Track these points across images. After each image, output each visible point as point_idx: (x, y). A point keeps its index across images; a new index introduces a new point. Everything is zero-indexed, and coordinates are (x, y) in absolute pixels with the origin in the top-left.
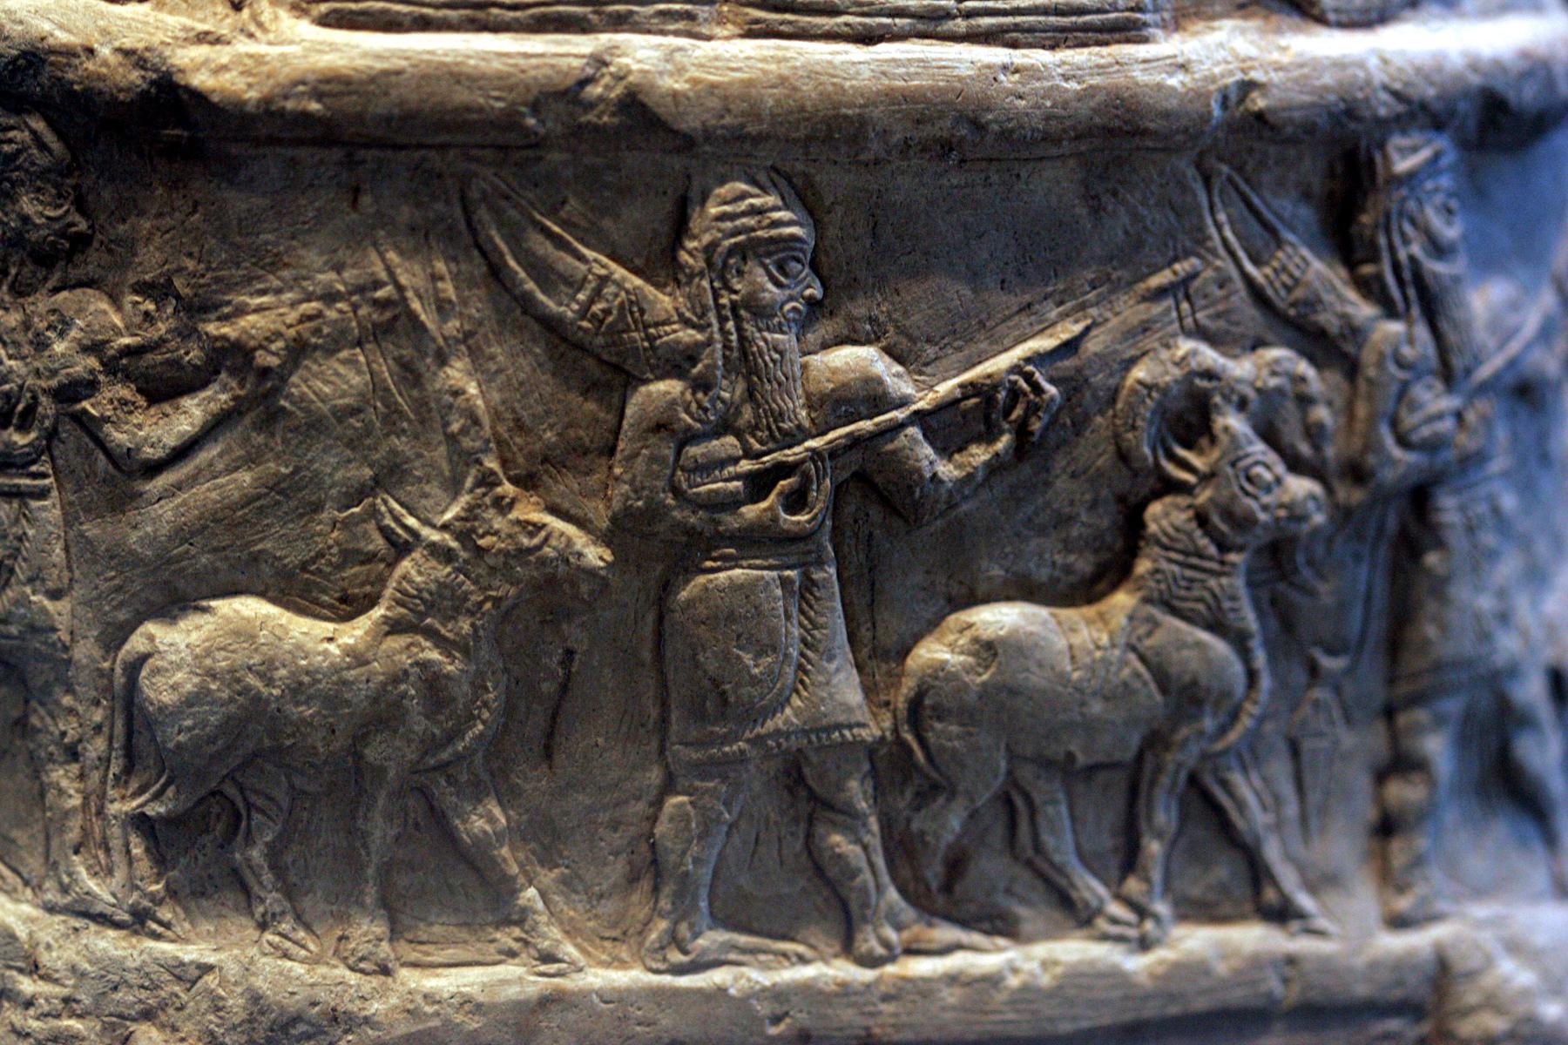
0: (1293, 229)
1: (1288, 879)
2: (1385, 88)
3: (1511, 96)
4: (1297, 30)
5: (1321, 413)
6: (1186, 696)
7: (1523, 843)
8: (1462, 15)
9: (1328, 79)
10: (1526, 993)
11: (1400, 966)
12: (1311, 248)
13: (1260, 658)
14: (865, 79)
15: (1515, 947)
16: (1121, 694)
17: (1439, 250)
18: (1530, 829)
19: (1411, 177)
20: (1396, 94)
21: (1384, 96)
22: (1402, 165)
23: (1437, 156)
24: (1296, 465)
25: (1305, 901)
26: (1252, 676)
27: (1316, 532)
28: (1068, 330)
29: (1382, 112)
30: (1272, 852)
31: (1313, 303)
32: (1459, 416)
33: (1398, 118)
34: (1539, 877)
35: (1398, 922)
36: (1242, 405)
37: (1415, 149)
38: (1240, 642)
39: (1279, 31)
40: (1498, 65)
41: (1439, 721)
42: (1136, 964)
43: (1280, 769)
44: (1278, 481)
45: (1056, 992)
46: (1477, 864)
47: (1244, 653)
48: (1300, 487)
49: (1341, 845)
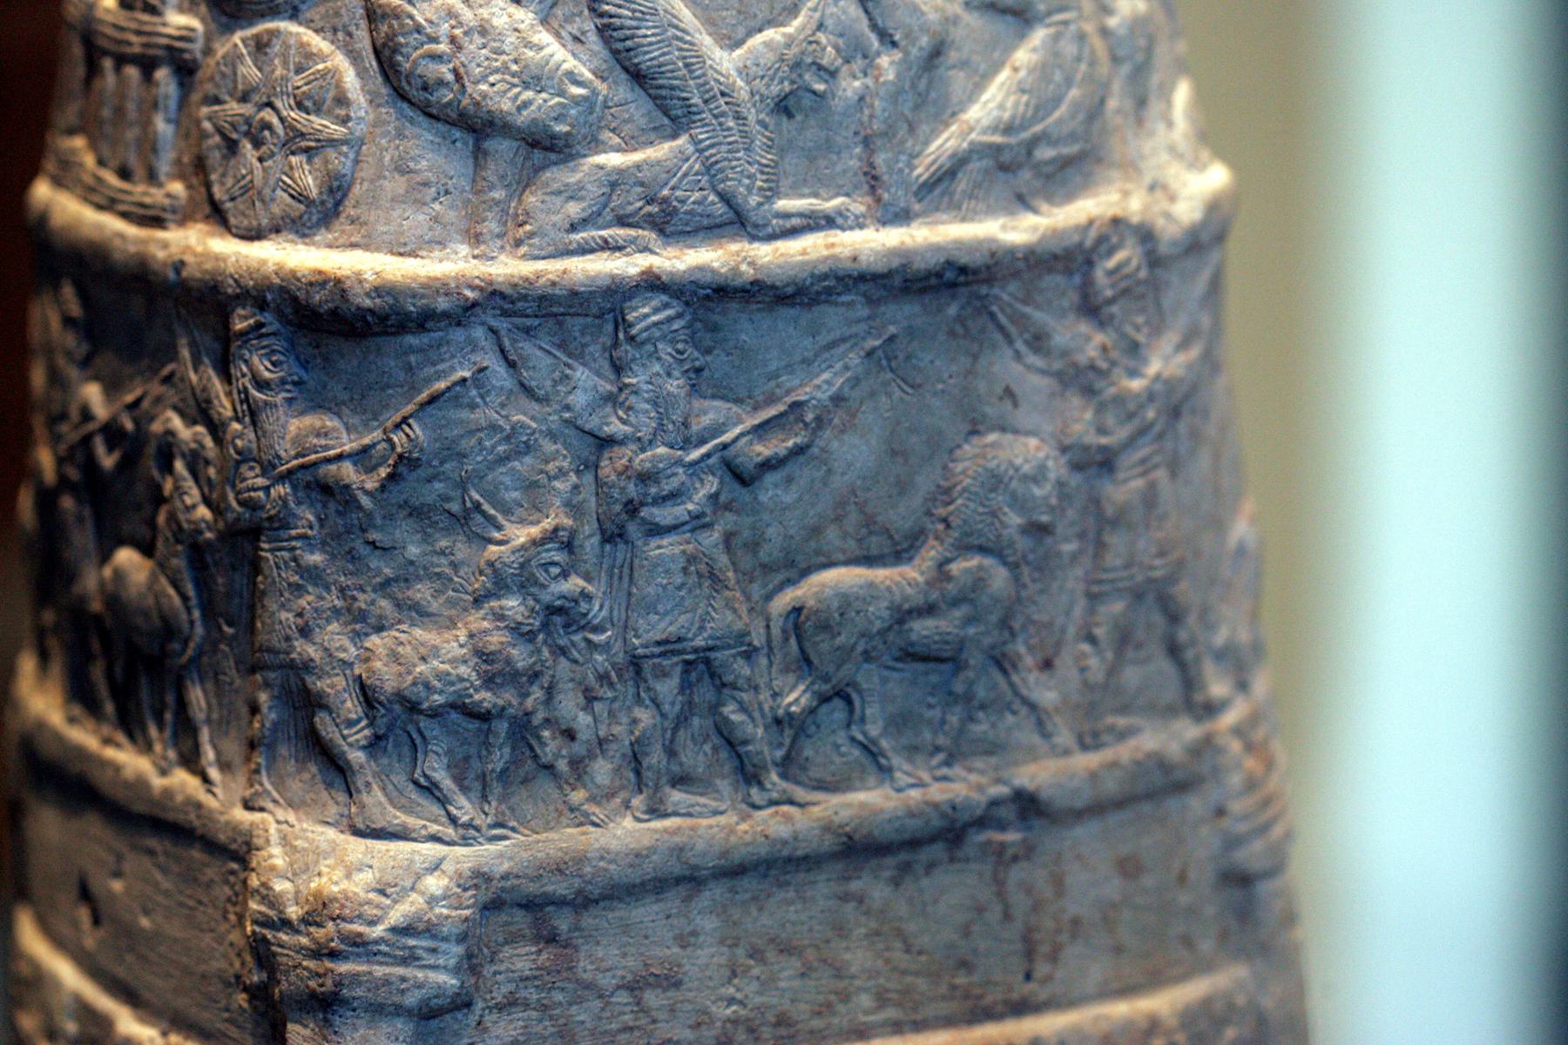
0: (208, 355)
1: (209, 754)
2: (232, 276)
3: (301, 295)
4: (221, 236)
5: (212, 472)
6: (169, 630)
7: (329, 785)
8: (314, 244)
9: (208, 266)
10: (273, 868)
11: (235, 828)
12: (215, 368)
13: (196, 614)
14: (87, 233)
15: (285, 841)
16: (146, 614)
17: (262, 385)
18: (338, 781)
19: (243, 334)
20: (236, 281)
21: (231, 282)
22: (239, 326)
23: (259, 325)
24: (207, 501)
25: (214, 773)
26: (192, 623)
27: (208, 543)
28: (138, 392)
29: (230, 291)
30: (205, 735)
31: (208, 401)
32: (267, 489)
33: (237, 296)
34: (333, 811)
35: (248, 806)
36: (183, 456)
37: (246, 318)
38: (185, 598)
39: (212, 235)
40: (293, 273)
41: (267, 685)
42: (157, 782)
43: (210, 685)
44: (194, 506)
45: (127, 785)
46: (295, 786)
47: (189, 610)
48: (203, 512)
49: (233, 749)
